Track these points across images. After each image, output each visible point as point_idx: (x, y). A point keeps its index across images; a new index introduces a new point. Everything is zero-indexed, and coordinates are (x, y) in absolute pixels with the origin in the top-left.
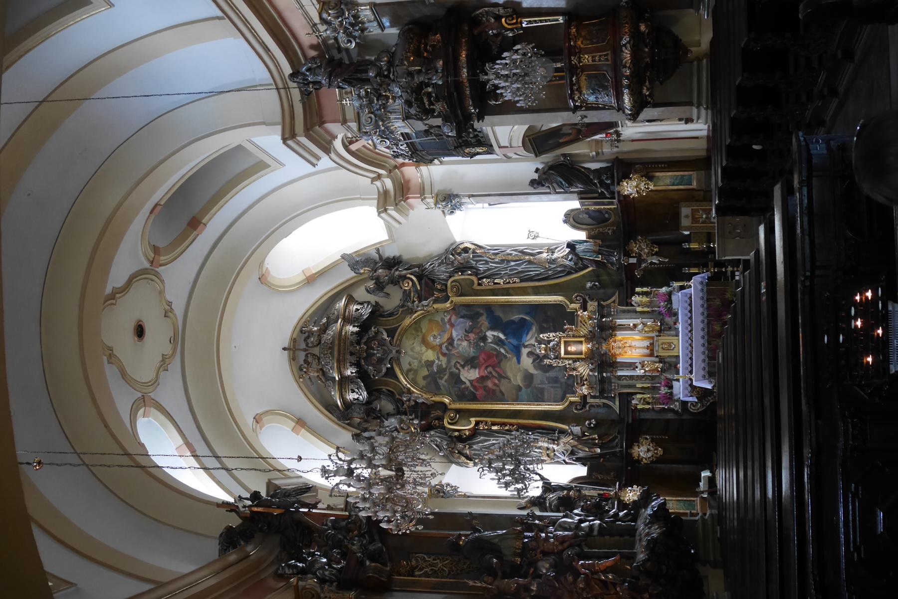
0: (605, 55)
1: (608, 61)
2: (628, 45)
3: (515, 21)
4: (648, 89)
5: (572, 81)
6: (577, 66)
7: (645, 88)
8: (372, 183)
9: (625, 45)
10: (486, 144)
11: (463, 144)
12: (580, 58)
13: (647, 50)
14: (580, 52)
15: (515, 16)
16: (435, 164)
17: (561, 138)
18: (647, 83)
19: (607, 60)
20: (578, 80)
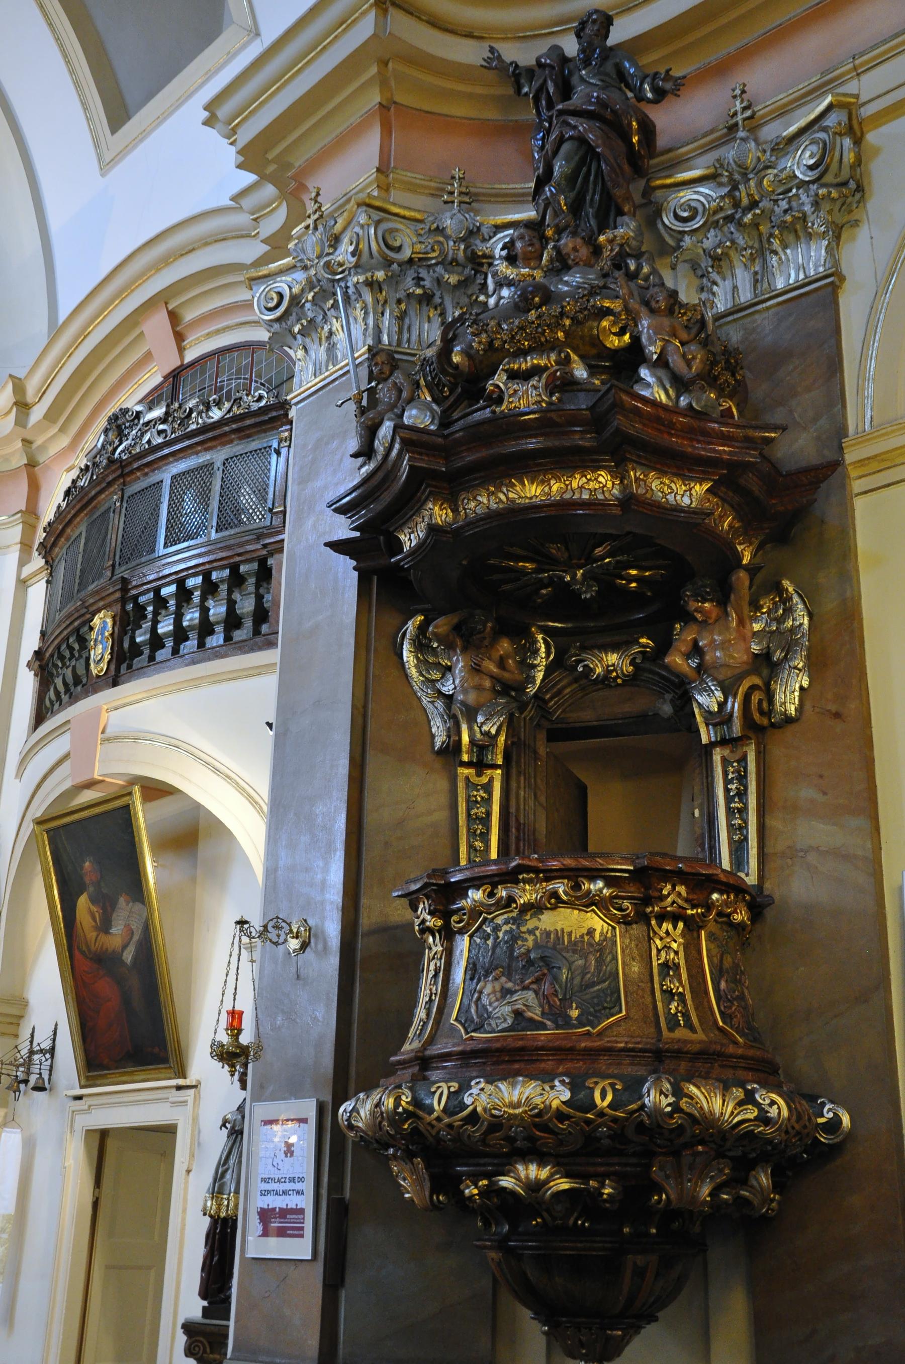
0: (686, 1016)
1: (671, 1030)
2: (752, 1113)
3: (756, 716)
4: (536, 1187)
5: (592, 879)
6: (647, 901)
7: (544, 1173)
8: (10, 376)
9: (749, 1099)
10: (118, 670)
11: (130, 606)
12: (675, 918)
13: (705, 1191)
14: (688, 920)
15: (765, 722)
16: (22, 563)
17: (93, 900)
18: (563, 1184)
19: (673, 1024)
20: (590, 902)
